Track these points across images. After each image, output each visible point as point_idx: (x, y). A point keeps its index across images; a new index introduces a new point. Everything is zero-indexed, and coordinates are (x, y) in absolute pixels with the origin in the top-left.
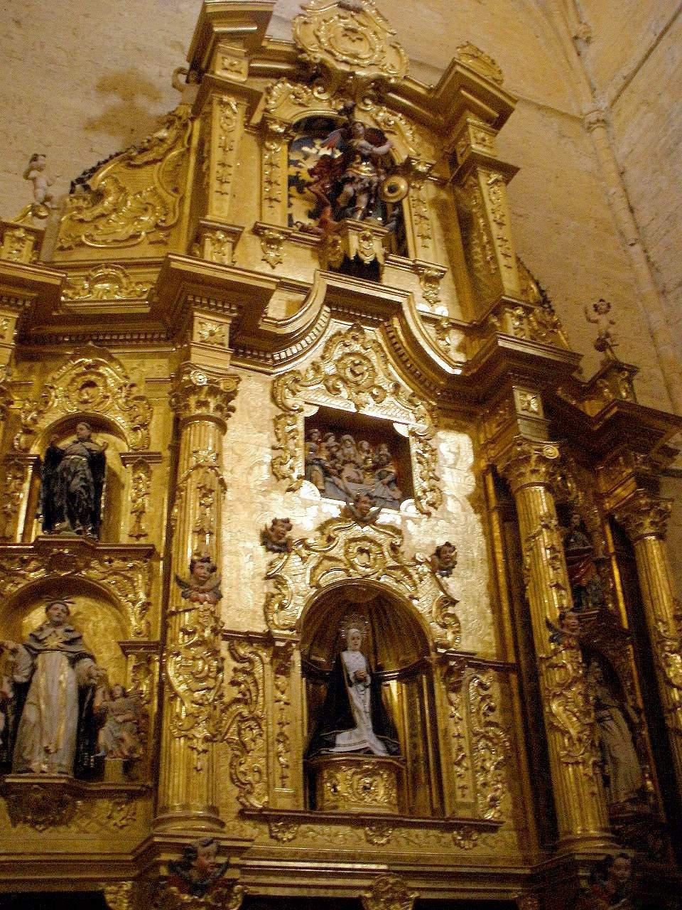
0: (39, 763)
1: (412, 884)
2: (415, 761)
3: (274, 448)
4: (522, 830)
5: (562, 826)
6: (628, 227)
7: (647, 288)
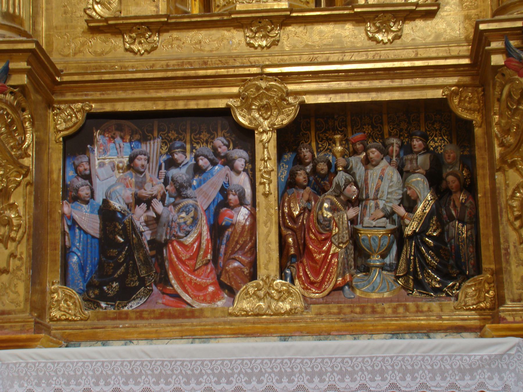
1: (291, 87)
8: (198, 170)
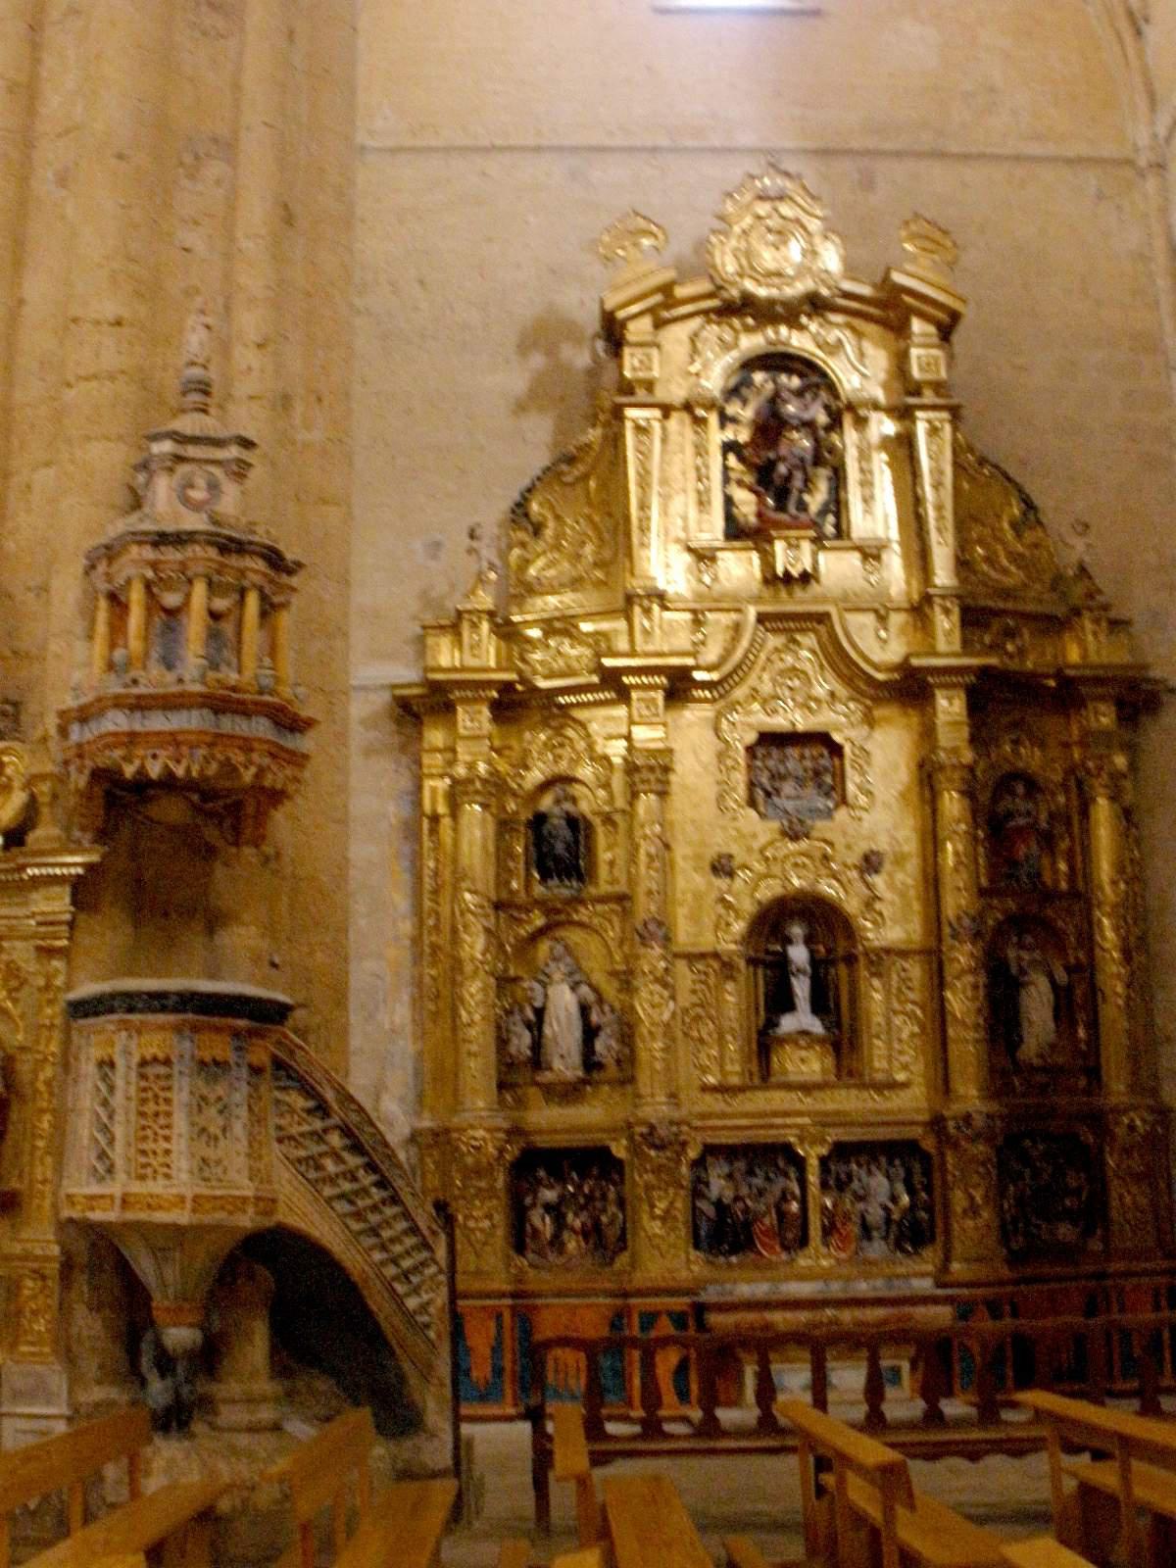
0: (557, 1064)
3: (718, 783)
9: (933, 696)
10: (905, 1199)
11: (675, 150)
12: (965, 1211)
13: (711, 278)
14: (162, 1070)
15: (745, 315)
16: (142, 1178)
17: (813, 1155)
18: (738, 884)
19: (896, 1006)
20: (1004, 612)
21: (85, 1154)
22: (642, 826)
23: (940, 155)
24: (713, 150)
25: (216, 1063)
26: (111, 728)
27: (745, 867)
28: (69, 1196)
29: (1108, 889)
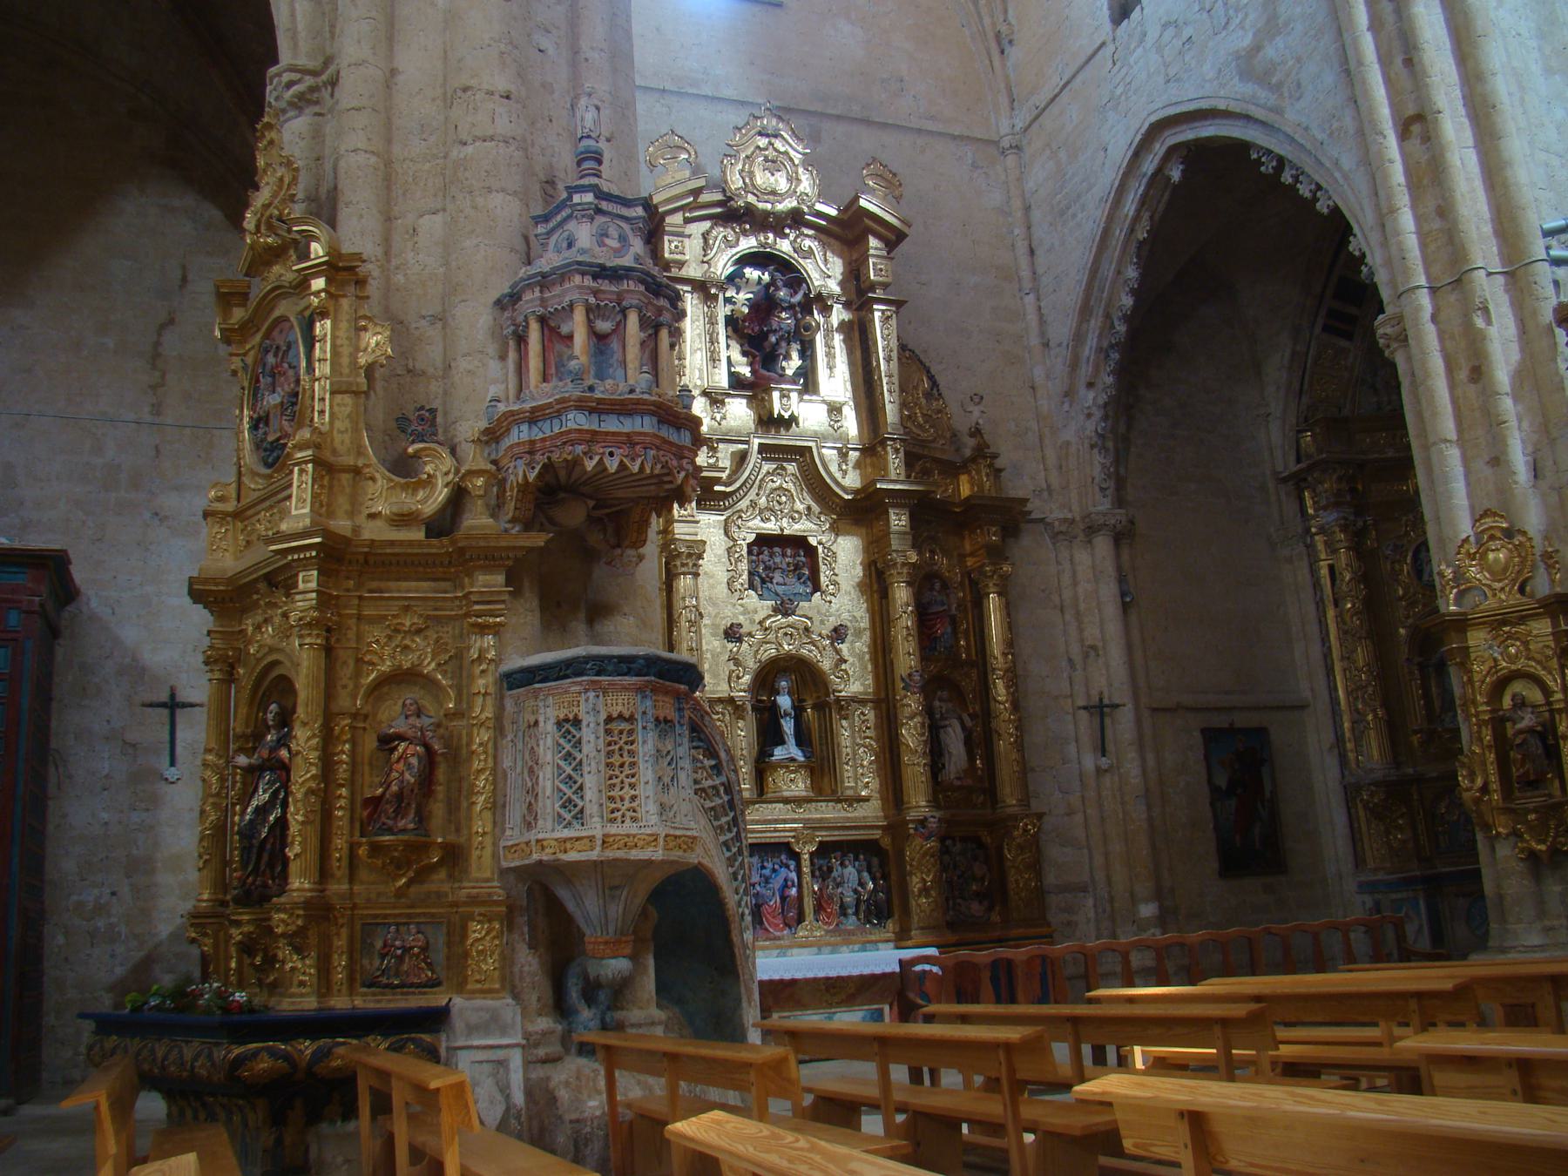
2: (822, 759)
4: (884, 799)
5: (906, 799)
6: (1025, 273)
7: (1034, 341)
8: (774, 870)
9: (887, 513)
10: (871, 885)
11: (680, 94)
12: (920, 891)
13: (724, 191)
14: (625, 726)
15: (745, 222)
16: (613, 821)
17: (806, 850)
18: (745, 645)
19: (858, 740)
20: (924, 456)
21: (548, 802)
22: (684, 599)
23: (867, 122)
24: (706, 97)
25: (666, 721)
26: (571, 425)
27: (750, 635)
28: (538, 841)
29: (1000, 659)
